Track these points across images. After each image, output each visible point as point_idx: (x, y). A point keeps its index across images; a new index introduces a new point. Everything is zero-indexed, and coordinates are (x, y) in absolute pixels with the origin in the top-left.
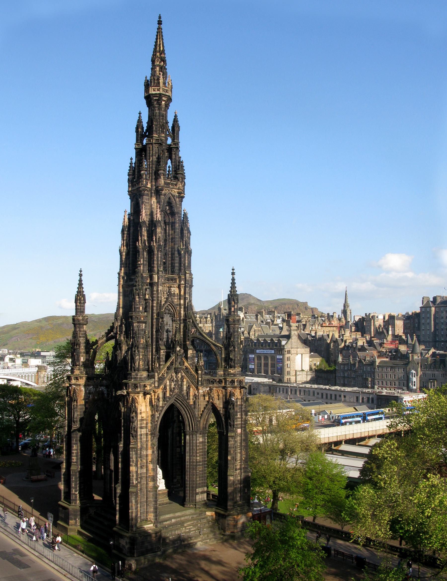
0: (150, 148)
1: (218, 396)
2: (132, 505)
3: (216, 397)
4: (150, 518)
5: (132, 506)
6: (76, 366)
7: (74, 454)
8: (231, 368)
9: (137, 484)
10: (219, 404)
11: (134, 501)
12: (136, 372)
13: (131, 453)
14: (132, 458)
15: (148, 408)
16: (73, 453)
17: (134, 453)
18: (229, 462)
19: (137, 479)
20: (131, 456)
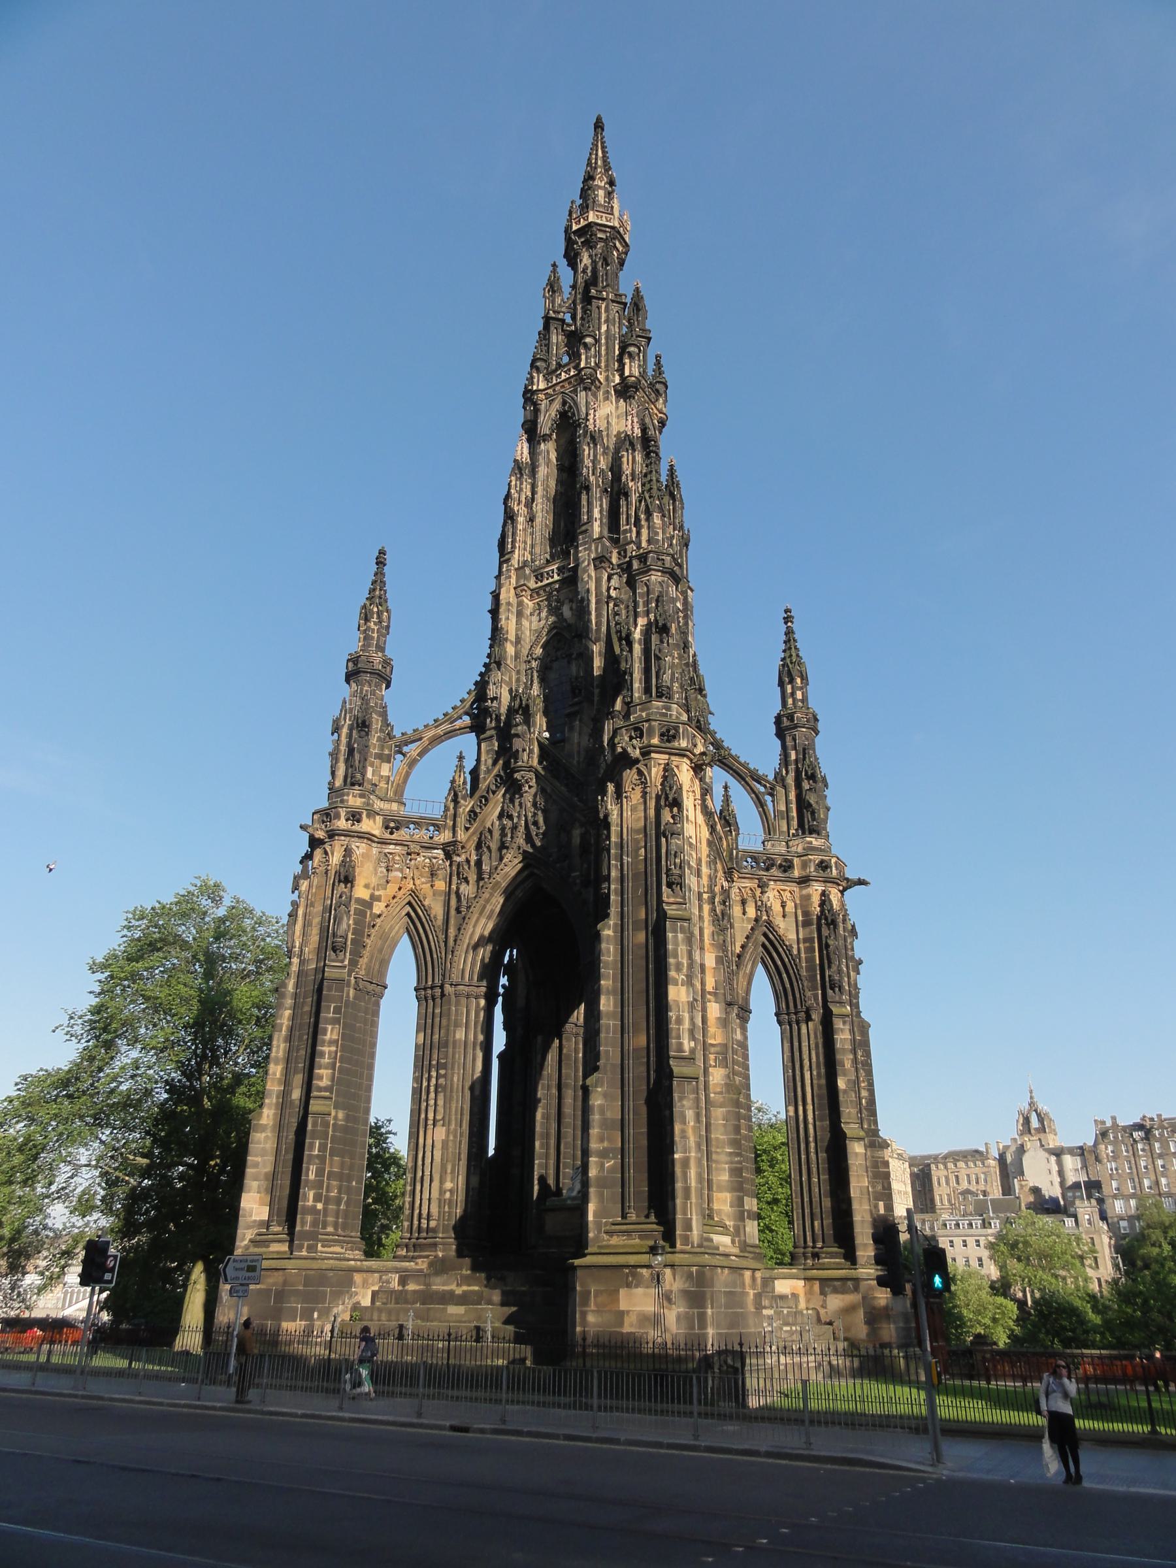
0: (599, 308)
1: (783, 907)
2: (683, 1131)
3: (777, 908)
4: (719, 1212)
5: (684, 1137)
6: (353, 784)
7: (326, 1060)
8: (810, 833)
9: (693, 1051)
10: (788, 930)
11: (690, 1114)
12: (664, 699)
13: (670, 935)
14: (676, 956)
15: (701, 819)
16: (322, 1054)
17: (680, 936)
18: (841, 1099)
19: (692, 1037)
20: (670, 947)
